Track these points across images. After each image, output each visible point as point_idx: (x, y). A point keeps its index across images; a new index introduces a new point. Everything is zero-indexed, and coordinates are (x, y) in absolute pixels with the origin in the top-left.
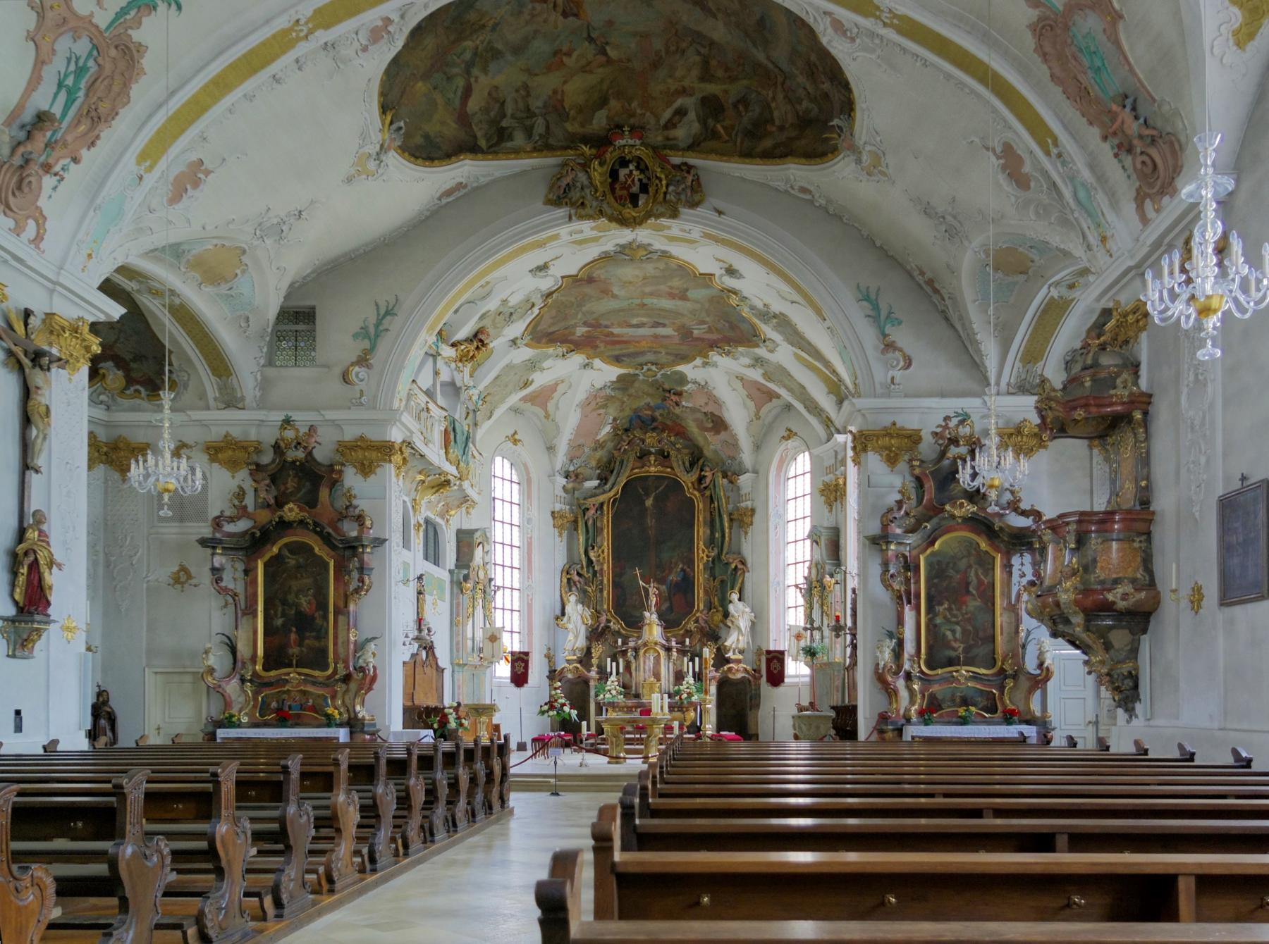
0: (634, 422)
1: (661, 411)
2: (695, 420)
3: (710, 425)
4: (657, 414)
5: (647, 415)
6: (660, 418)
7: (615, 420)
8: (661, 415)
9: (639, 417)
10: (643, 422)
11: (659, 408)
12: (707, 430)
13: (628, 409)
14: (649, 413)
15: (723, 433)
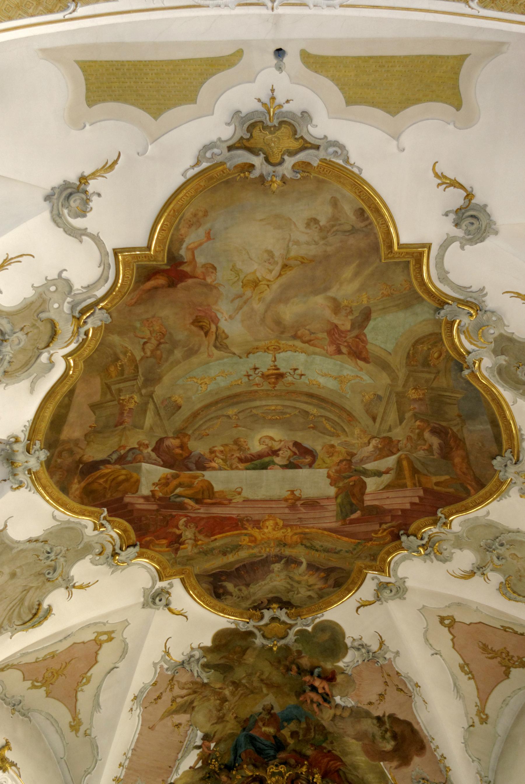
0: (241, 751)
1: (293, 726)
2: (360, 737)
3: (389, 746)
4: (286, 732)
5: (267, 735)
6: (291, 741)
7: (206, 737)
8: (294, 734)
9: (252, 740)
10: (259, 751)
11: (289, 720)
12: (384, 756)
13: (230, 717)
14: (270, 730)
15: (416, 760)
